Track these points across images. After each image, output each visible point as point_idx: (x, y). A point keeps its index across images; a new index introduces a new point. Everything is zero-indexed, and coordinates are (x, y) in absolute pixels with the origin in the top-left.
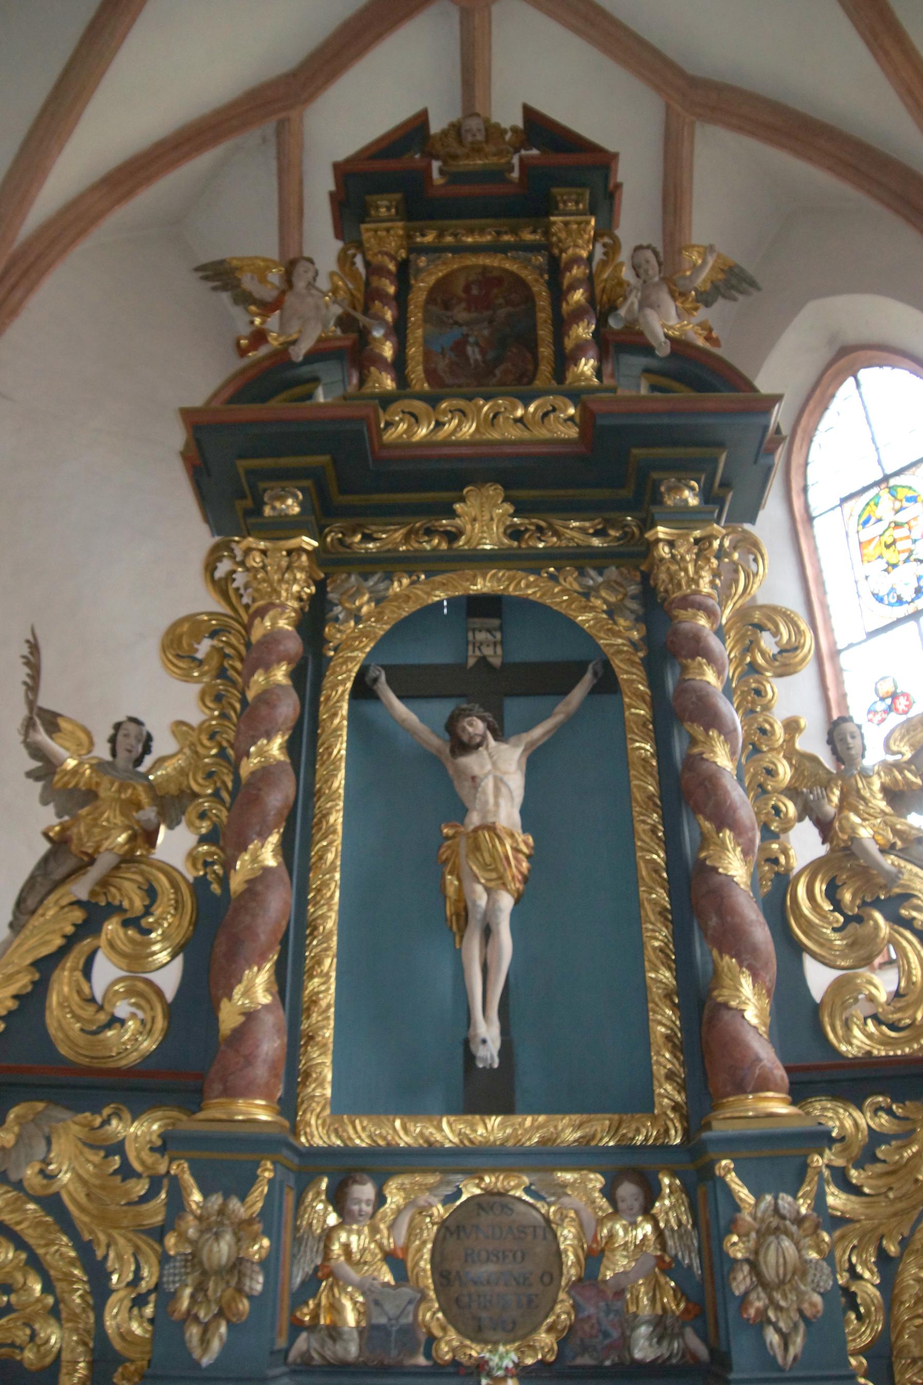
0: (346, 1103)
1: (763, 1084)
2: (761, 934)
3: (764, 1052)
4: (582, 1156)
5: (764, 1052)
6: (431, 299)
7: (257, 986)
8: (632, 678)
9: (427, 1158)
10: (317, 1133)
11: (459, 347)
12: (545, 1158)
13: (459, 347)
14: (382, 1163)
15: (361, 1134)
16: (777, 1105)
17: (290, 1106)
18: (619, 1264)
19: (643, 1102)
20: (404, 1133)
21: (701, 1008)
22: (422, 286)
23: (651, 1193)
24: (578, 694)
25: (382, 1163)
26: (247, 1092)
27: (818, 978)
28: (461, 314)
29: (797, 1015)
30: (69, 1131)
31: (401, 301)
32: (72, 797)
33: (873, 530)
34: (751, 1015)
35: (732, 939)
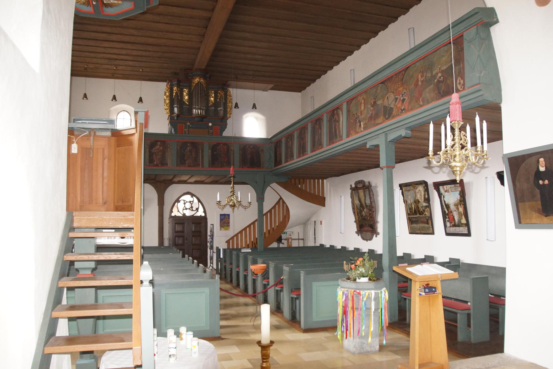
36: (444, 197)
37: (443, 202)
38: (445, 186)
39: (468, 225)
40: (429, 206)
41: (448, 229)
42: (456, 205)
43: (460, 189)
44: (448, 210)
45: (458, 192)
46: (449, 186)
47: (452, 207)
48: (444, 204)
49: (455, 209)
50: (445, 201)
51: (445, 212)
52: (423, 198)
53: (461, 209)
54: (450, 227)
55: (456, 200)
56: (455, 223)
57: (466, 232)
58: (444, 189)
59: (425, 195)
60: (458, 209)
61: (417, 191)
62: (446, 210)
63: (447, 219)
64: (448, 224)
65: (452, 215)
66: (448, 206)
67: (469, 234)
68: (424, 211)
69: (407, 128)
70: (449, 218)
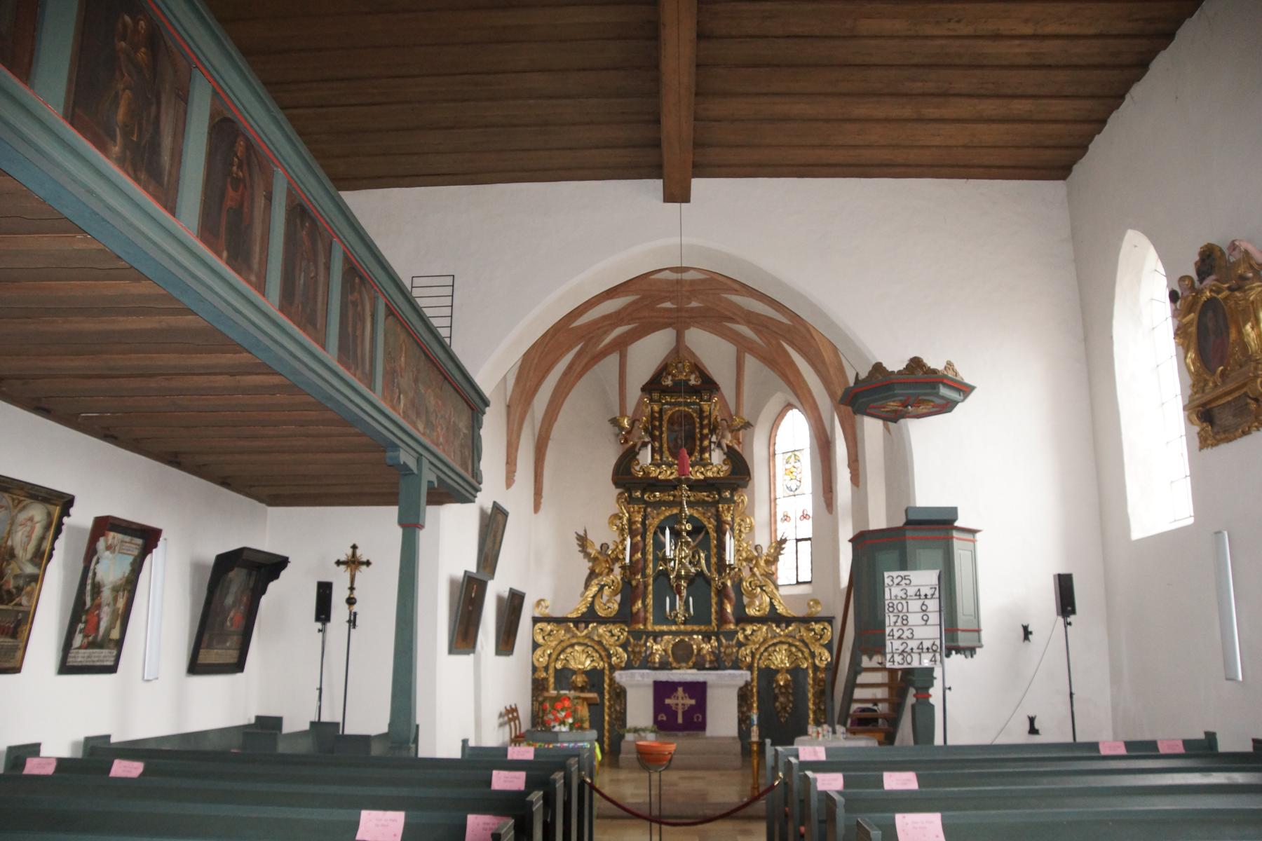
0: (655, 623)
1: (728, 622)
2: (732, 595)
3: (731, 618)
4: (698, 633)
5: (731, 618)
6: (668, 421)
7: (639, 604)
8: (713, 534)
9: (669, 633)
10: (650, 628)
11: (676, 439)
12: (693, 632)
13: (676, 439)
14: (663, 633)
15: (657, 628)
16: (732, 627)
17: (645, 625)
18: (704, 652)
19: (710, 623)
20: (665, 628)
21: (721, 610)
22: (666, 418)
23: (710, 639)
24: (701, 536)
25: (663, 633)
26: (638, 622)
27: (746, 600)
28: (676, 428)
29: (740, 608)
30: (601, 630)
31: (661, 425)
32: (595, 560)
33: (788, 466)
34: (729, 610)
35: (727, 597)
36: (98, 562)
37: (90, 574)
38: (112, 534)
39: (119, 644)
40: (36, 579)
41: (73, 653)
42: (116, 590)
43: (136, 553)
44: (93, 599)
45: (131, 559)
46: (120, 536)
47: (106, 594)
48: (89, 581)
49: (110, 600)
50: (95, 574)
51: (84, 603)
52: (31, 548)
53: (121, 603)
54: (80, 648)
55: (120, 576)
56: (96, 637)
57: (110, 663)
58: (106, 541)
59: (42, 539)
60: (115, 600)
61: (22, 517)
62: (88, 599)
63: (81, 626)
64: (78, 640)
65: (98, 615)
66: (97, 588)
67: (112, 669)
68: (19, 590)
69: (438, 477)
70: (86, 622)
